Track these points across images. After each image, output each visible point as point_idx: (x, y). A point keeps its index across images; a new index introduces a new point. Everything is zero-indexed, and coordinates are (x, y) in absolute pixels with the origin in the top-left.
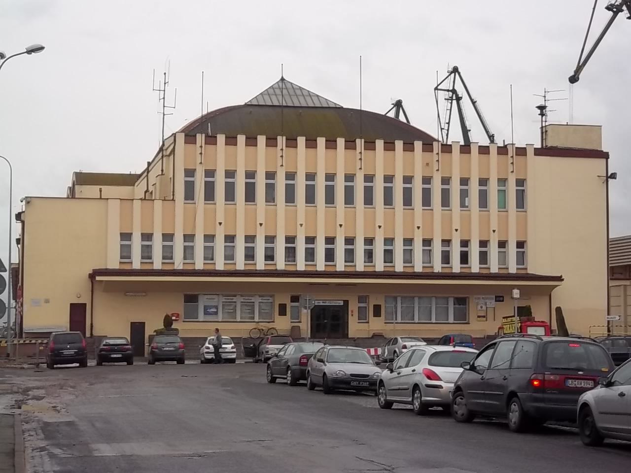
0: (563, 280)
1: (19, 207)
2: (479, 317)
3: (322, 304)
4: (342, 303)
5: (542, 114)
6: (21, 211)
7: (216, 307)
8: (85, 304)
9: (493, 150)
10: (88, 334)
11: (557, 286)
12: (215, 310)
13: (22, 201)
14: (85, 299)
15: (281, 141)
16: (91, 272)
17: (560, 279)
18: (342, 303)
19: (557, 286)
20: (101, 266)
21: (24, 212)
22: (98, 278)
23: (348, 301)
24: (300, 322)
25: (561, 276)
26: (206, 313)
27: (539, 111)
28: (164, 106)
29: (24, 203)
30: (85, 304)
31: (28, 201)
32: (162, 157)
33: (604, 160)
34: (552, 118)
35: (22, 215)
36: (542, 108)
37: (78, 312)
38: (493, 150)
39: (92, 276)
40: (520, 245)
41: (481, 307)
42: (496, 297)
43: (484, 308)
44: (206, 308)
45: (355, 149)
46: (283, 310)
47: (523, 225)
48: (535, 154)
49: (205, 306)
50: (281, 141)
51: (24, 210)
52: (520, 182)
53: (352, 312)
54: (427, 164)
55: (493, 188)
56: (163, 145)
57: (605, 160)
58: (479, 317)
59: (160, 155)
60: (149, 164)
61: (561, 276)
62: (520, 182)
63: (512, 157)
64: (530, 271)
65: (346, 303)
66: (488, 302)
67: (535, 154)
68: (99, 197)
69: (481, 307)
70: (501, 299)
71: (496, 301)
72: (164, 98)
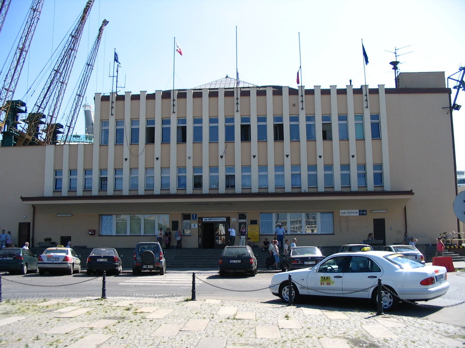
0: (413, 194)
3: (208, 220)
5: (395, 68)
11: (410, 199)
17: (410, 193)
25: (411, 191)
27: (393, 67)
33: (447, 95)
34: (402, 69)
36: (395, 64)
38: (350, 93)
45: (234, 96)
57: (447, 95)
61: (411, 191)
63: (366, 95)
70: (361, 213)
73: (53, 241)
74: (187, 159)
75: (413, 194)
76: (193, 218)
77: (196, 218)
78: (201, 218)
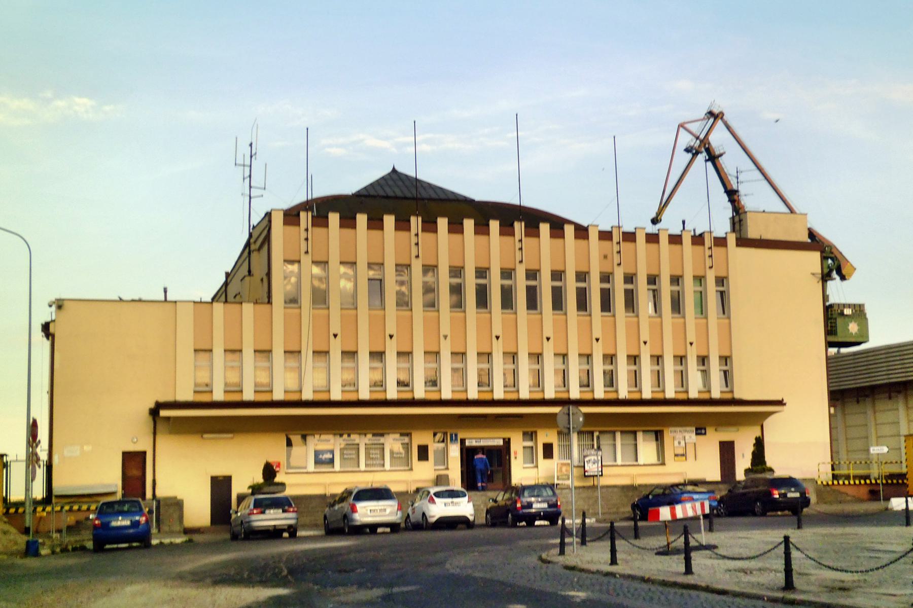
0: (785, 404)
1: (44, 314)
2: (676, 455)
4: (501, 443)
6: (49, 320)
7: (332, 452)
8: (144, 453)
9: (687, 240)
10: (149, 495)
12: (331, 456)
13: (50, 306)
14: (143, 444)
15: (416, 222)
16: (152, 405)
17: (780, 403)
18: (501, 443)
19: (770, 414)
20: (169, 398)
21: (53, 321)
22: (164, 413)
23: (509, 439)
24: (447, 469)
26: (318, 462)
28: (250, 187)
29: (54, 308)
30: (144, 453)
31: (59, 305)
32: (249, 253)
35: (51, 326)
37: (134, 463)
39: (154, 412)
40: (725, 359)
41: (679, 443)
42: (697, 429)
43: (683, 443)
44: (317, 453)
46: (423, 453)
47: (727, 335)
48: (737, 245)
49: (315, 452)
50: (416, 222)
51: (54, 318)
52: (721, 281)
53: (516, 453)
54: (605, 257)
55: (689, 288)
56: (251, 235)
58: (676, 455)
59: (247, 250)
60: (228, 275)
62: (721, 281)
64: (738, 395)
65: (507, 442)
66: (687, 436)
67: (737, 245)
68: (163, 299)
69: (679, 443)
70: (703, 431)
71: (697, 434)
72: (250, 176)
73: (260, 479)
74: (442, 338)
75: (785, 404)
76: (452, 439)
77: (456, 439)
78: (463, 441)
